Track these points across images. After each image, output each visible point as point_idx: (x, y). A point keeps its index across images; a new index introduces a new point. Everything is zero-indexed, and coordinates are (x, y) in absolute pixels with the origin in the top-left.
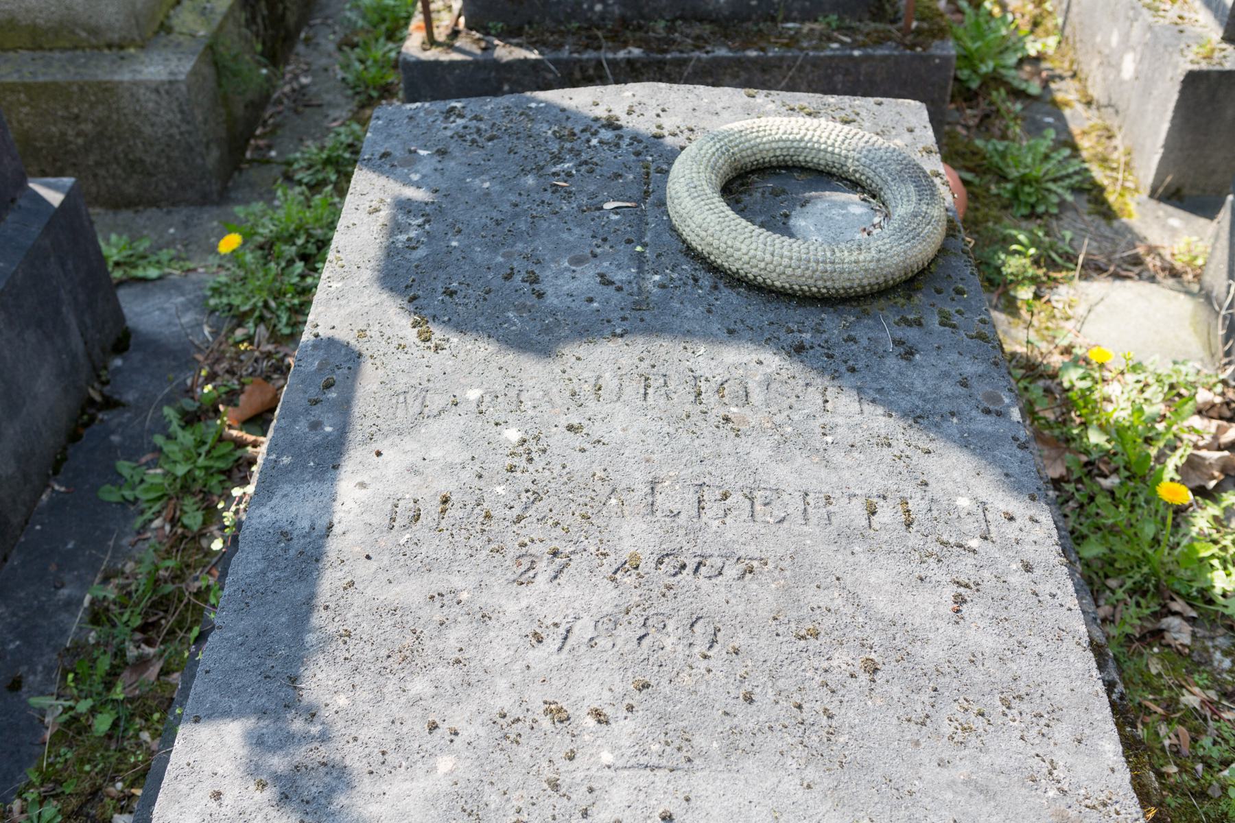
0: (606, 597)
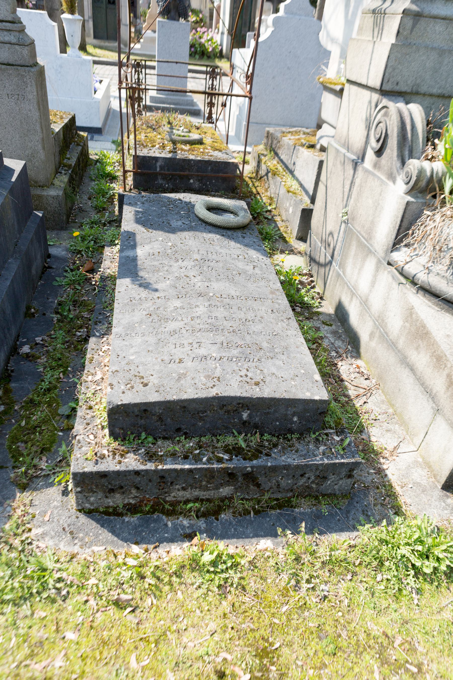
0: (193, 264)
